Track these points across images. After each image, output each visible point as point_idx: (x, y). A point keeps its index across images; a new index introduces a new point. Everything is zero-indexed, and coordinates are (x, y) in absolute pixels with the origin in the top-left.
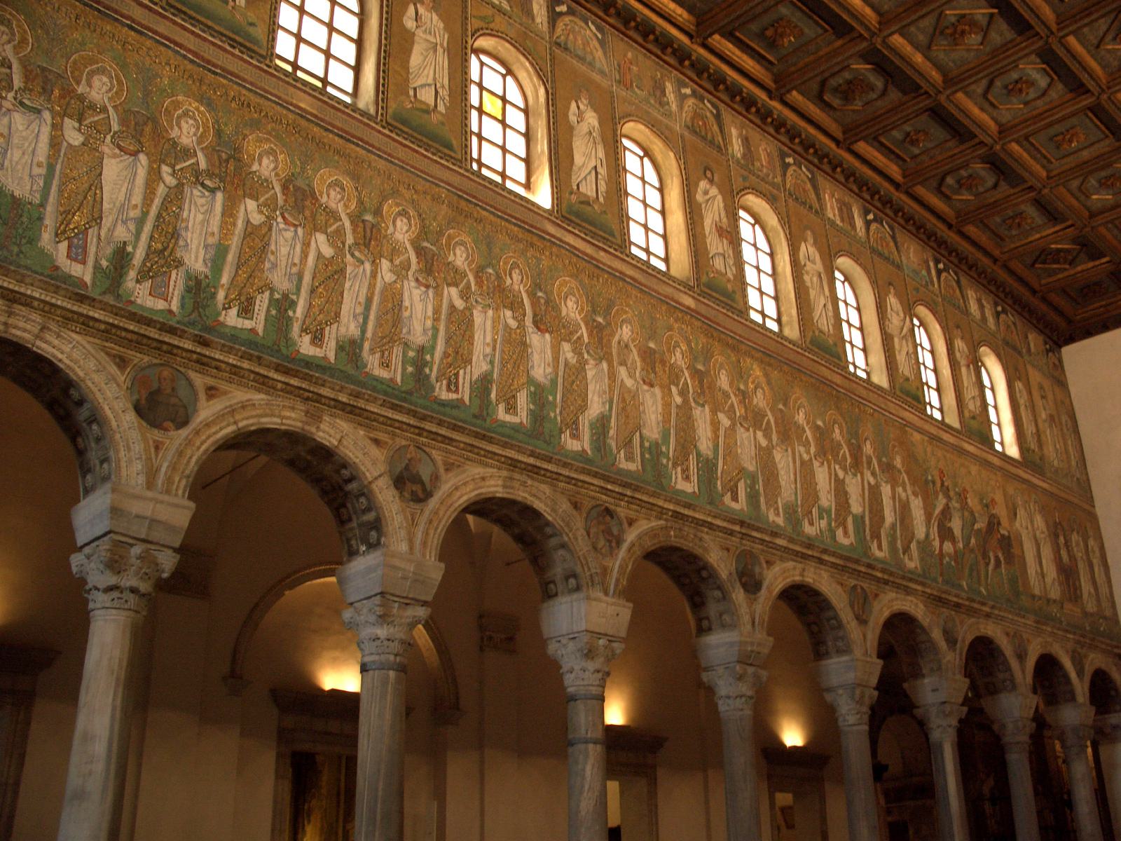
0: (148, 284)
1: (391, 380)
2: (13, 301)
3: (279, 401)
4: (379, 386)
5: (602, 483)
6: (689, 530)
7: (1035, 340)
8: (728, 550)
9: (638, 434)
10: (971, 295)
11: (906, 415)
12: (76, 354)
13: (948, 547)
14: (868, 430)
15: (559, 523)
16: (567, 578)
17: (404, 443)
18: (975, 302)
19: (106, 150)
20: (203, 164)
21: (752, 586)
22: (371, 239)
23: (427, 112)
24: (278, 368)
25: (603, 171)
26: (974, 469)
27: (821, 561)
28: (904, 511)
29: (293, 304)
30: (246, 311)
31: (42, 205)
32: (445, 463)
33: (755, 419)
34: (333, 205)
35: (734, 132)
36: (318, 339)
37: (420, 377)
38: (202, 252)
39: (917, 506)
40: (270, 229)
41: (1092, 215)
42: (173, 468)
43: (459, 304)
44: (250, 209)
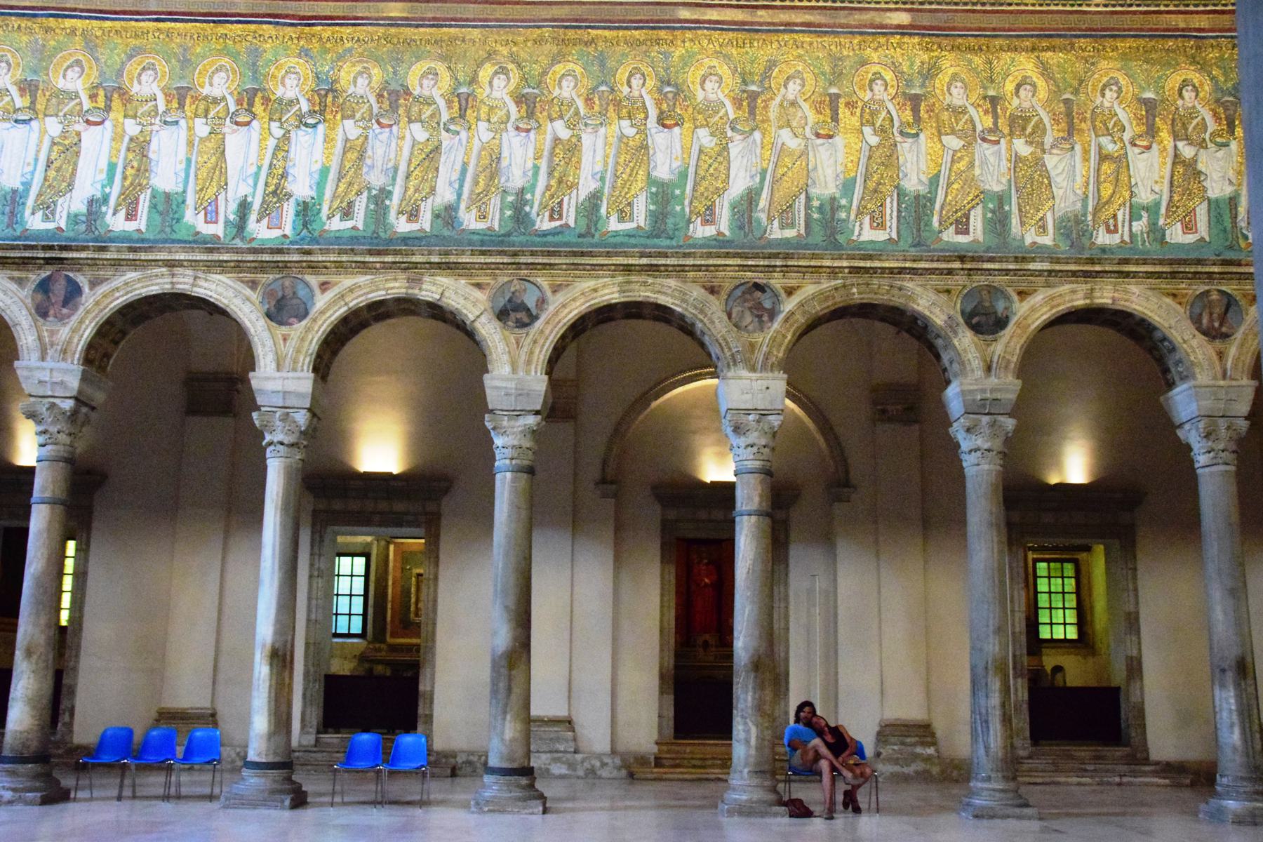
0: (265, 221)
1: (489, 229)
2: (174, 266)
3: (380, 278)
4: (476, 237)
5: (739, 261)
8: (948, 291)
9: (803, 196)
12: (220, 289)
17: (506, 279)
19: (225, 130)
20: (305, 106)
24: (370, 253)
29: (390, 193)
30: (347, 213)
31: (184, 192)
32: (551, 286)
34: (426, 93)
37: (520, 216)
38: (308, 180)
40: (366, 138)
42: (298, 351)
44: (351, 129)
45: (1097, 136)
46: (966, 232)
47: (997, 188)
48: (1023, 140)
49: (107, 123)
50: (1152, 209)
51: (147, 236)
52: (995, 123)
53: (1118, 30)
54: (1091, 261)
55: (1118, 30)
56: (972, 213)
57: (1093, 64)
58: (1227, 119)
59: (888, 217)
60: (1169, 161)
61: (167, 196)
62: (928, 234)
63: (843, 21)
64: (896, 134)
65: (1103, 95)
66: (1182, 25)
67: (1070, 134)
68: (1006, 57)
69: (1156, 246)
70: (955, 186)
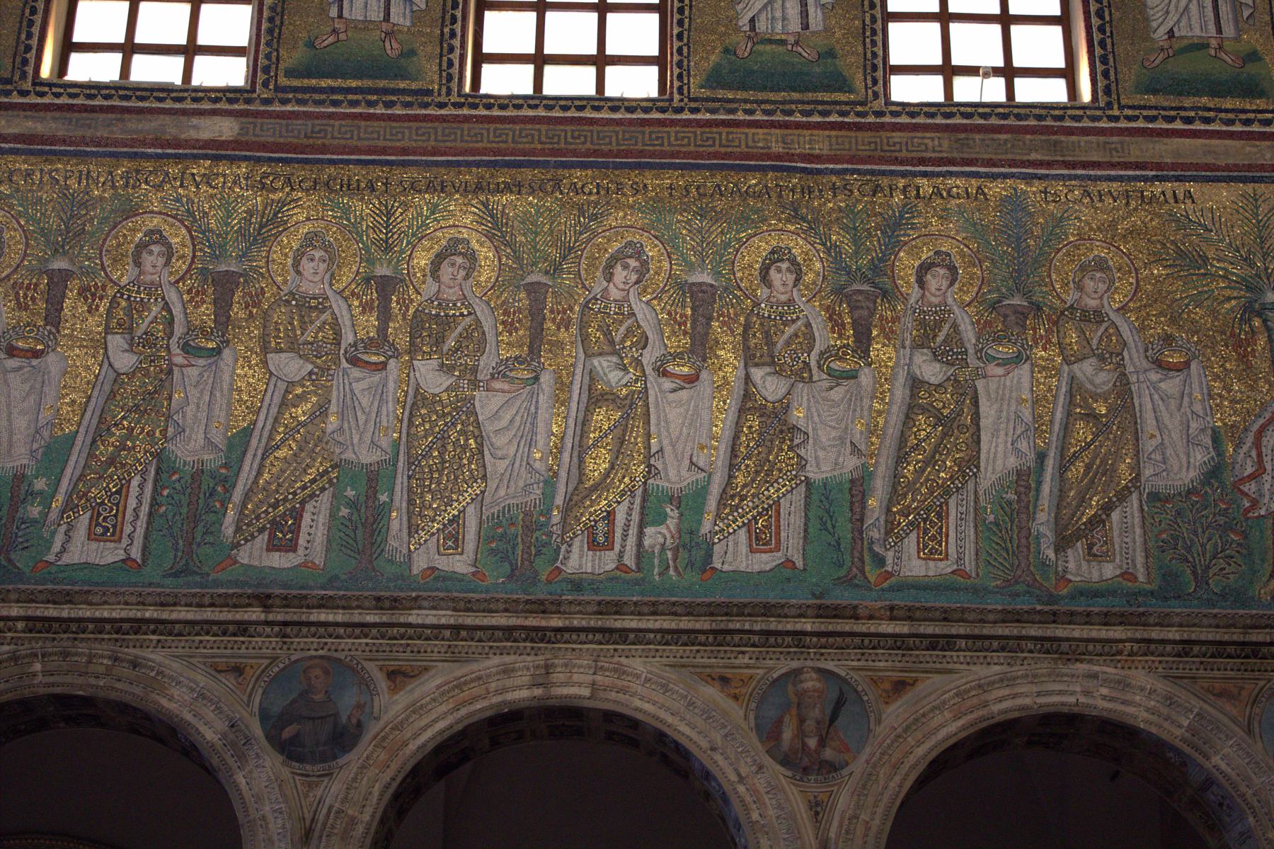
8: (238, 670)
45: (588, 356)
46: (292, 547)
47: (368, 457)
48: (434, 363)
50: (689, 502)
52: (382, 330)
53: (652, 155)
54: (541, 608)
55: (652, 155)
56: (309, 507)
57: (594, 217)
58: (854, 324)
59: (129, 515)
60: (732, 404)
62: (208, 550)
63: (102, 133)
64: (175, 350)
65: (609, 278)
66: (777, 148)
67: (534, 351)
68: (421, 201)
69: (692, 577)
70: (281, 453)
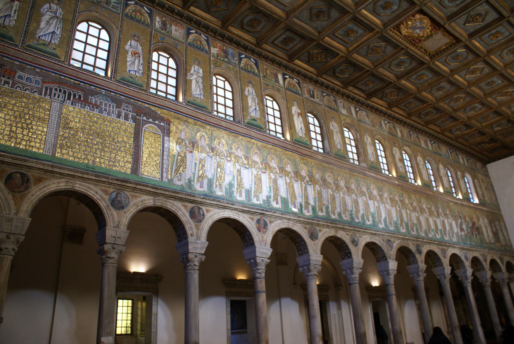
6: (406, 242)
7: (479, 165)
10: (460, 157)
11: (448, 198)
13: (463, 233)
14: (440, 205)
15: (381, 245)
16: (383, 257)
18: (462, 159)
20: (308, 180)
21: (420, 252)
22: (337, 187)
23: (340, 151)
25: (374, 153)
26: (467, 209)
27: (434, 243)
28: (451, 225)
33: (414, 209)
35: (398, 130)
36: (334, 214)
37: (352, 218)
39: (454, 223)
41: (495, 133)
43: (355, 198)
49: (267, 173)
51: (282, 210)
61: (284, 198)
